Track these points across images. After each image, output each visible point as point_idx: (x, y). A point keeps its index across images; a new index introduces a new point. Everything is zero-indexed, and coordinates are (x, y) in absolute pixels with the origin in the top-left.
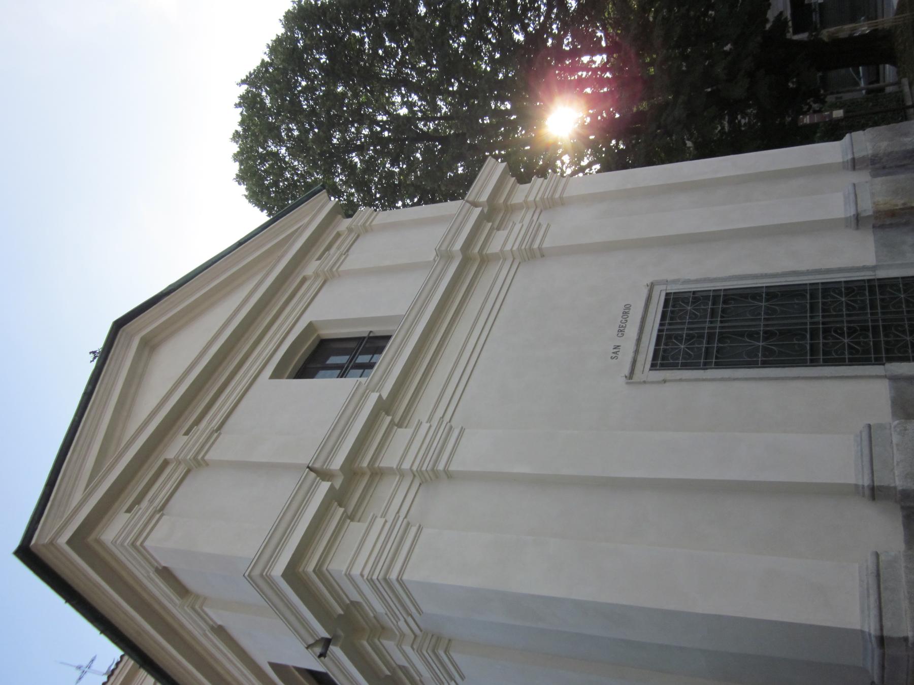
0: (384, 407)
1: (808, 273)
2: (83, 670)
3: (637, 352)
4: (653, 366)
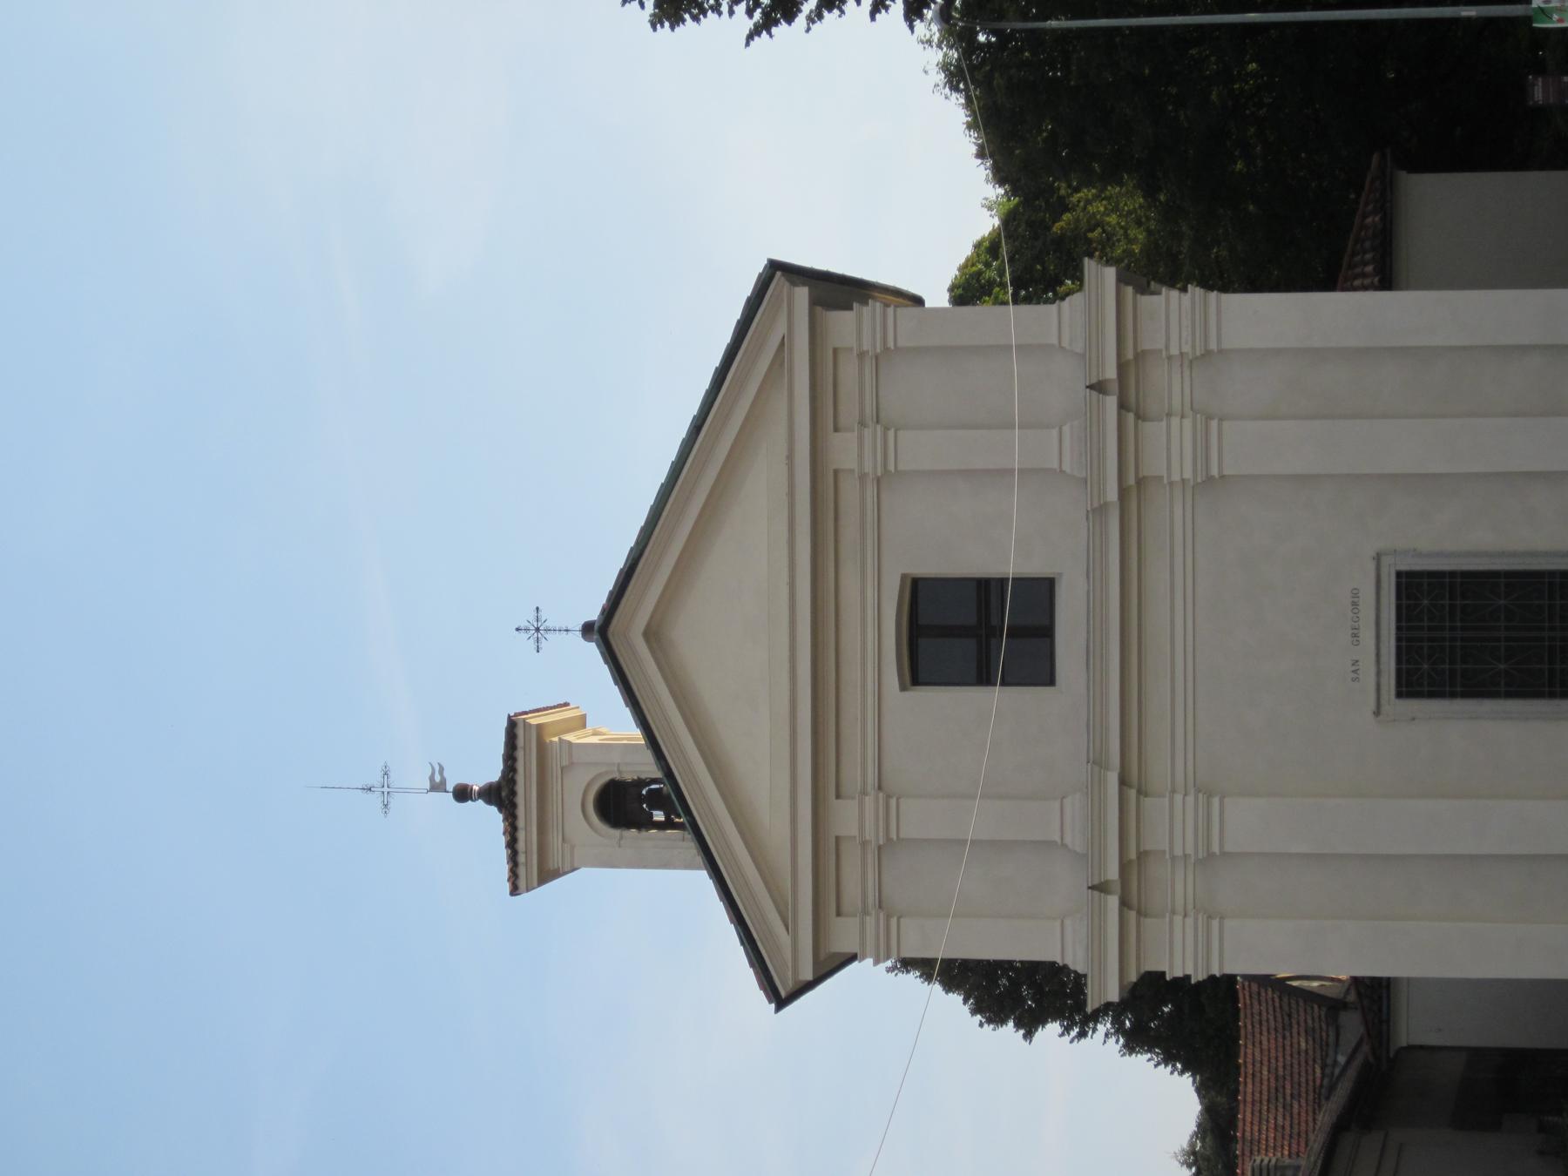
0: (1123, 782)
1: (1546, 554)
2: (383, 790)
3: (1378, 673)
4: (1399, 695)
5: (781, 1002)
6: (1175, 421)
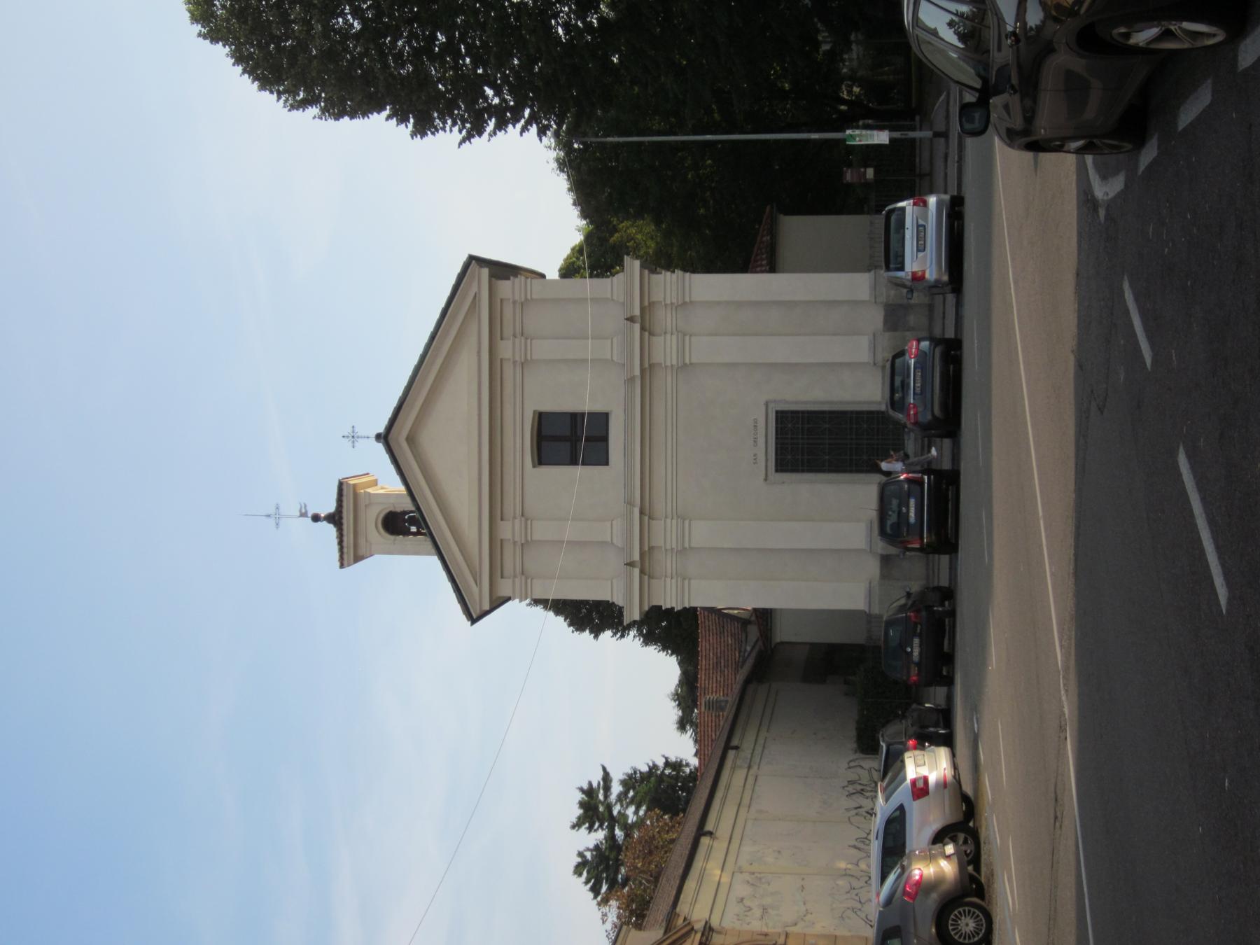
0: (642, 513)
3: (767, 460)
4: (777, 471)
5: (473, 620)
6: (668, 336)
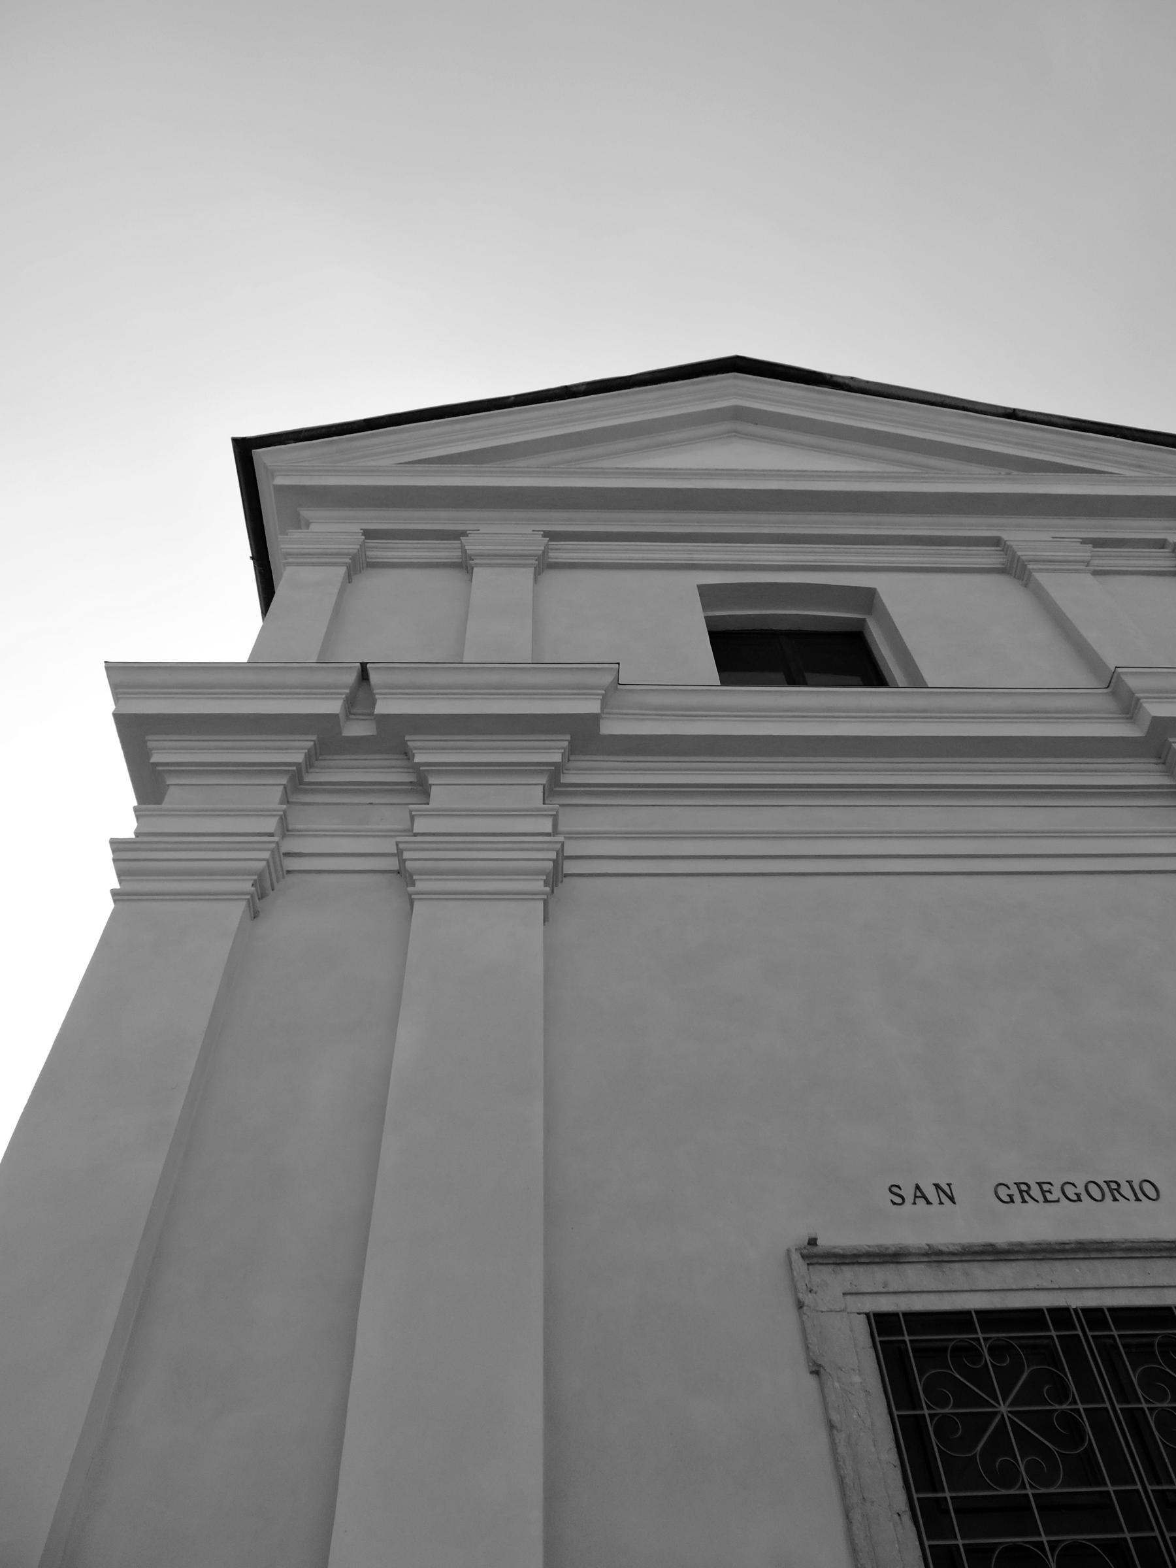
3: (935, 1257)
4: (882, 1323)
